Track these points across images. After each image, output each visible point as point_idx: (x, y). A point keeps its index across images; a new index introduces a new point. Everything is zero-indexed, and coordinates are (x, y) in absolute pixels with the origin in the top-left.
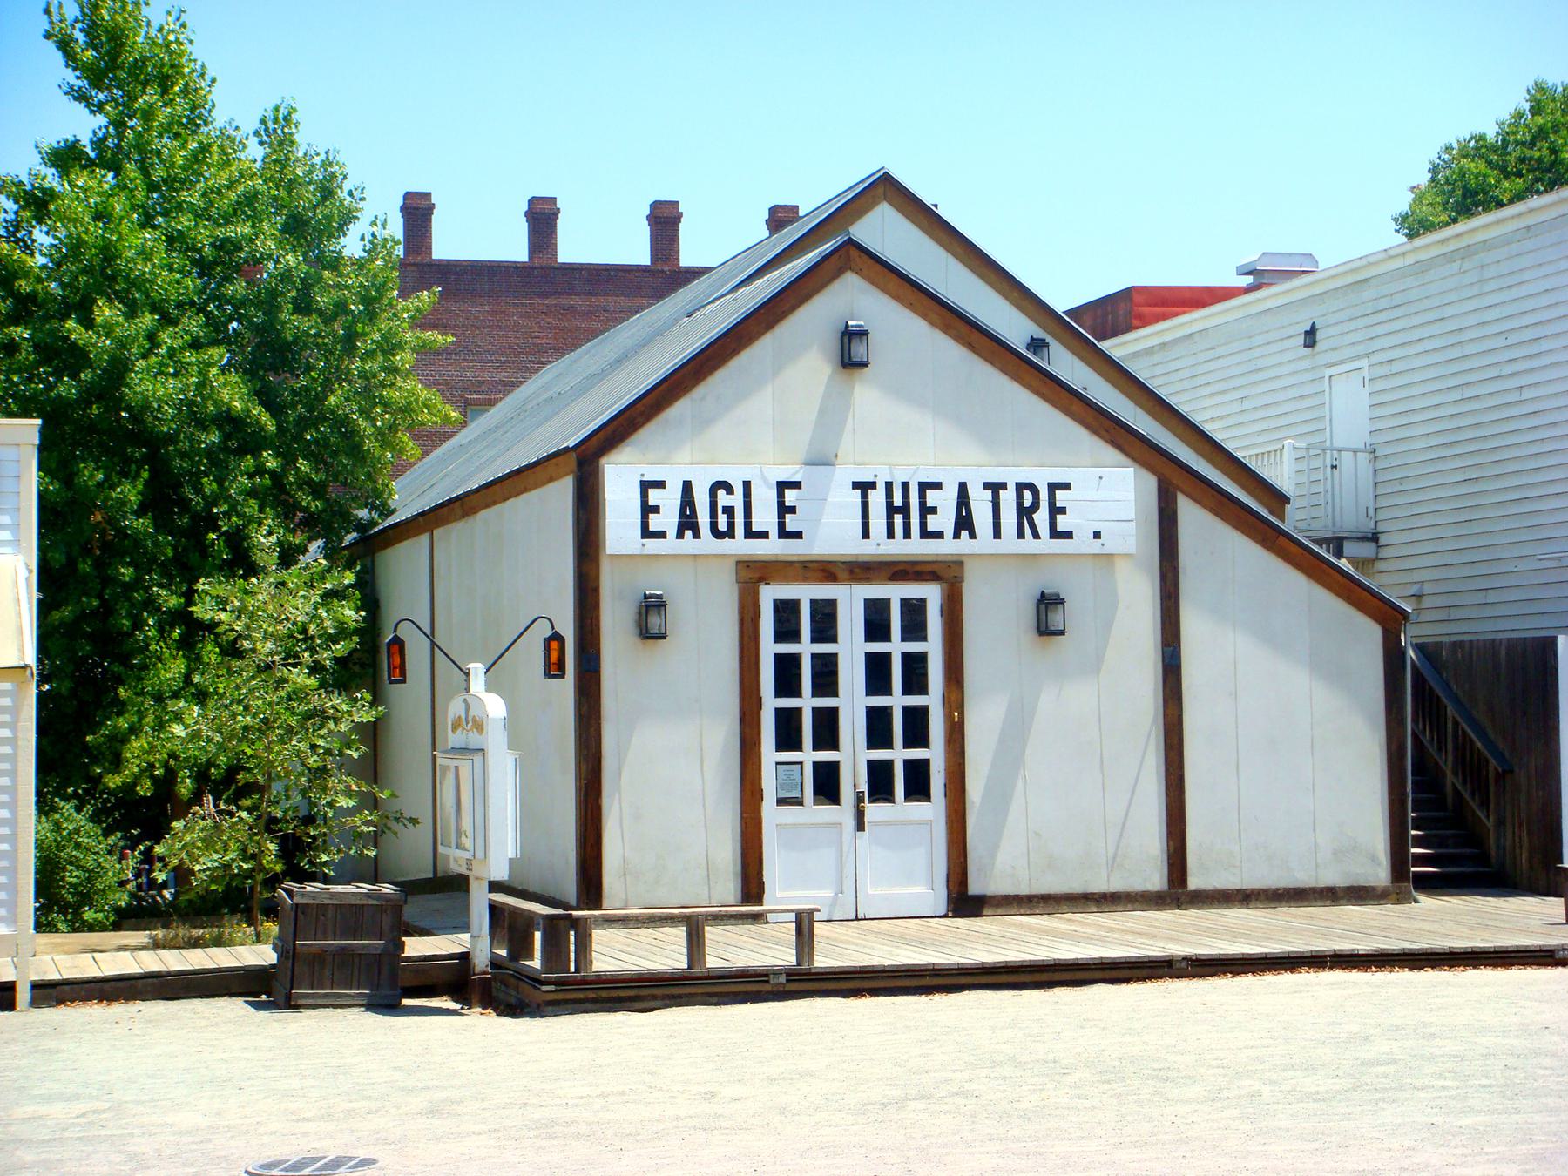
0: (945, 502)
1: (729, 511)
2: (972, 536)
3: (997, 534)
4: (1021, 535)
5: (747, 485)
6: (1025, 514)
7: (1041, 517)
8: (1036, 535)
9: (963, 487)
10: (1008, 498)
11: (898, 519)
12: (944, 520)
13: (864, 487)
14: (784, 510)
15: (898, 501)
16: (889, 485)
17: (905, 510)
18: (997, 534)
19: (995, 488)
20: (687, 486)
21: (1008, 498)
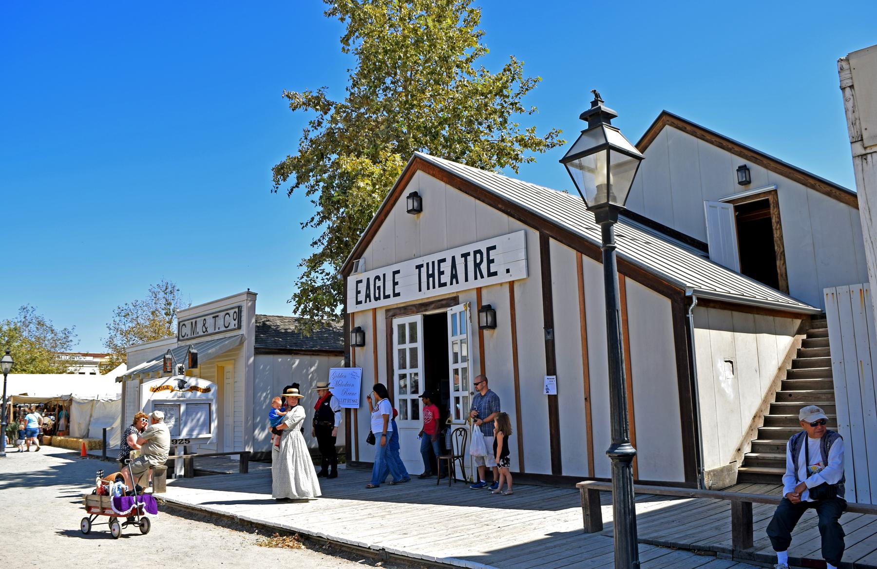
0: (446, 267)
1: (379, 288)
2: (457, 283)
3: (466, 280)
4: (476, 278)
5: (384, 275)
6: (477, 266)
7: (484, 267)
8: (482, 277)
9: (453, 258)
10: (470, 259)
11: (431, 279)
12: (446, 278)
13: (419, 267)
14: (395, 284)
15: (430, 272)
16: (428, 264)
17: (433, 275)
18: (466, 280)
19: (465, 256)
20: (368, 279)
21: (470, 259)
